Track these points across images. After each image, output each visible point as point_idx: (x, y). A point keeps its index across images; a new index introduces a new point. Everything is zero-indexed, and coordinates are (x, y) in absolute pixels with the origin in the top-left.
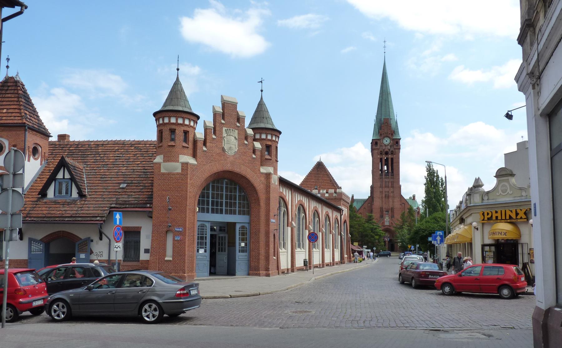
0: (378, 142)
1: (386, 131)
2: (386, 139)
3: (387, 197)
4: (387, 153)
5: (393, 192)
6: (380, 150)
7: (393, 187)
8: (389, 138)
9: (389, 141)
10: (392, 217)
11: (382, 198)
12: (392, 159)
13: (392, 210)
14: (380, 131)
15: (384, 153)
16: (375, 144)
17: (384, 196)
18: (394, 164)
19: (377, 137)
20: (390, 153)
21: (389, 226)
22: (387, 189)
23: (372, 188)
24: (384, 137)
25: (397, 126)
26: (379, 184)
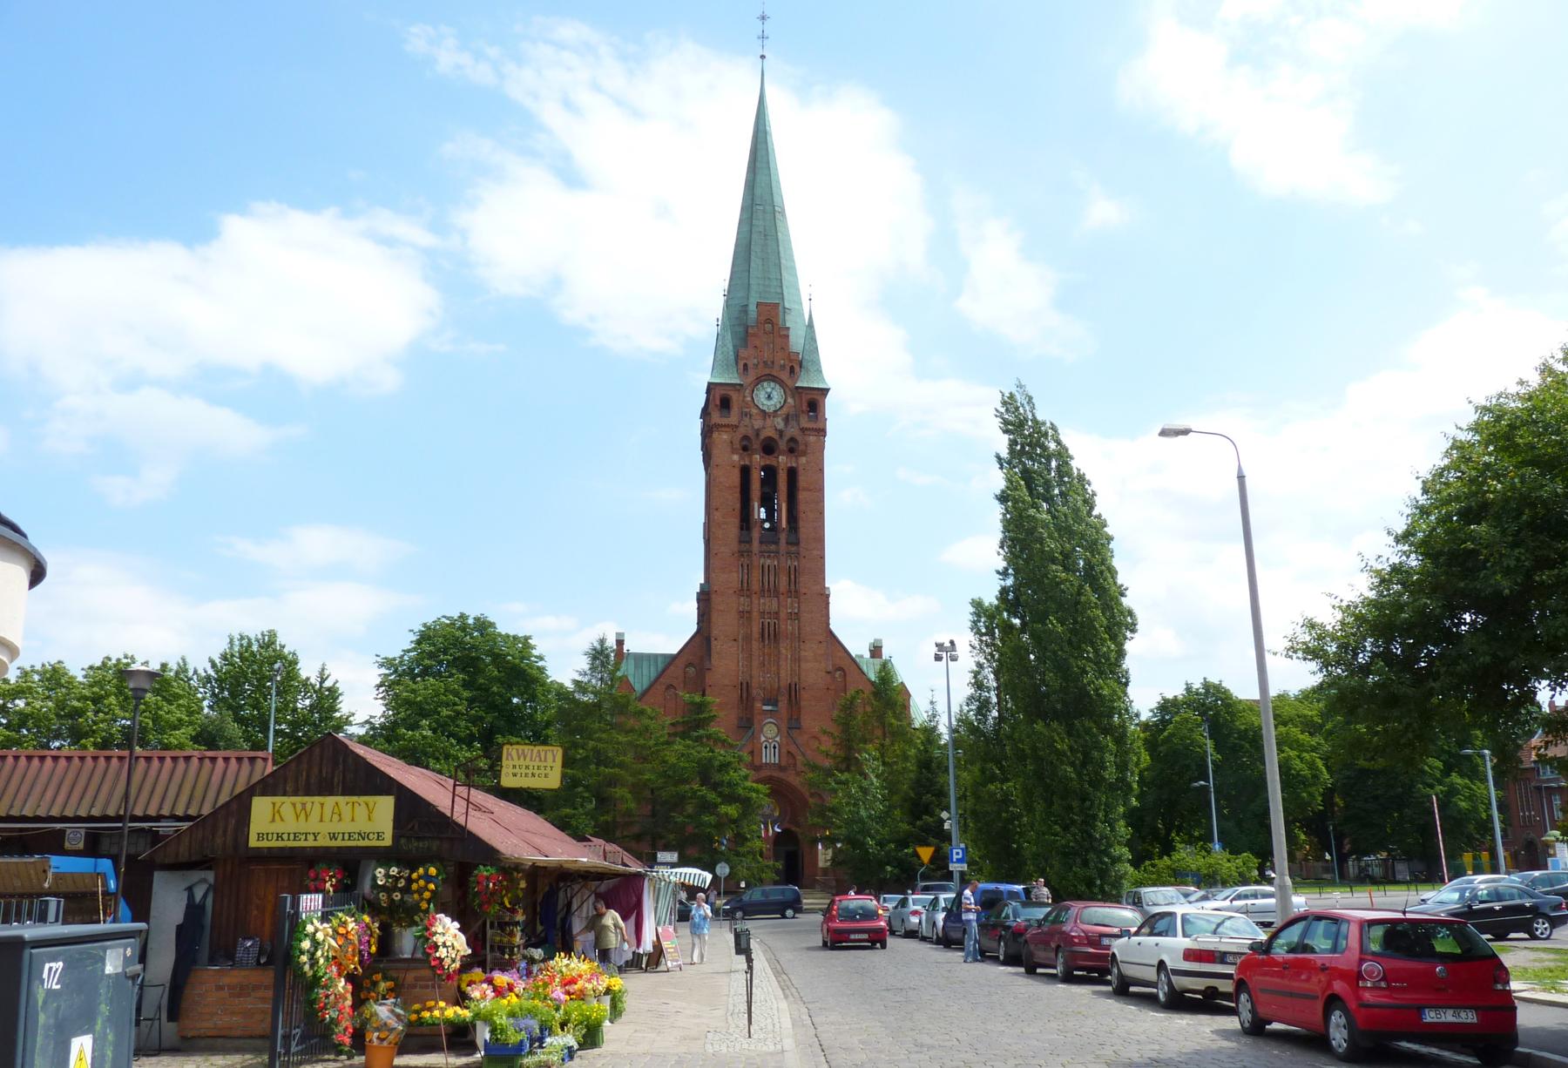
0: (734, 396)
1: (766, 355)
2: (768, 387)
3: (771, 635)
4: (769, 448)
5: (796, 616)
6: (742, 431)
7: (794, 592)
8: (782, 384)
9: (778, 395)
10: (793, 724)
11: (748, 639)
12: (792, 474)
13: (793, 692)
14: (743, 353)
15: (756, 445)
16: (719, 402)
17: (756, 629)
18: (802, 496)
19: (732, 378)
20: (783, 445)
21: (780, 767)
22: (771, 604)
23: (704, 598)
24: (759, 380)
25: (814, 340)
26: (734, 578)
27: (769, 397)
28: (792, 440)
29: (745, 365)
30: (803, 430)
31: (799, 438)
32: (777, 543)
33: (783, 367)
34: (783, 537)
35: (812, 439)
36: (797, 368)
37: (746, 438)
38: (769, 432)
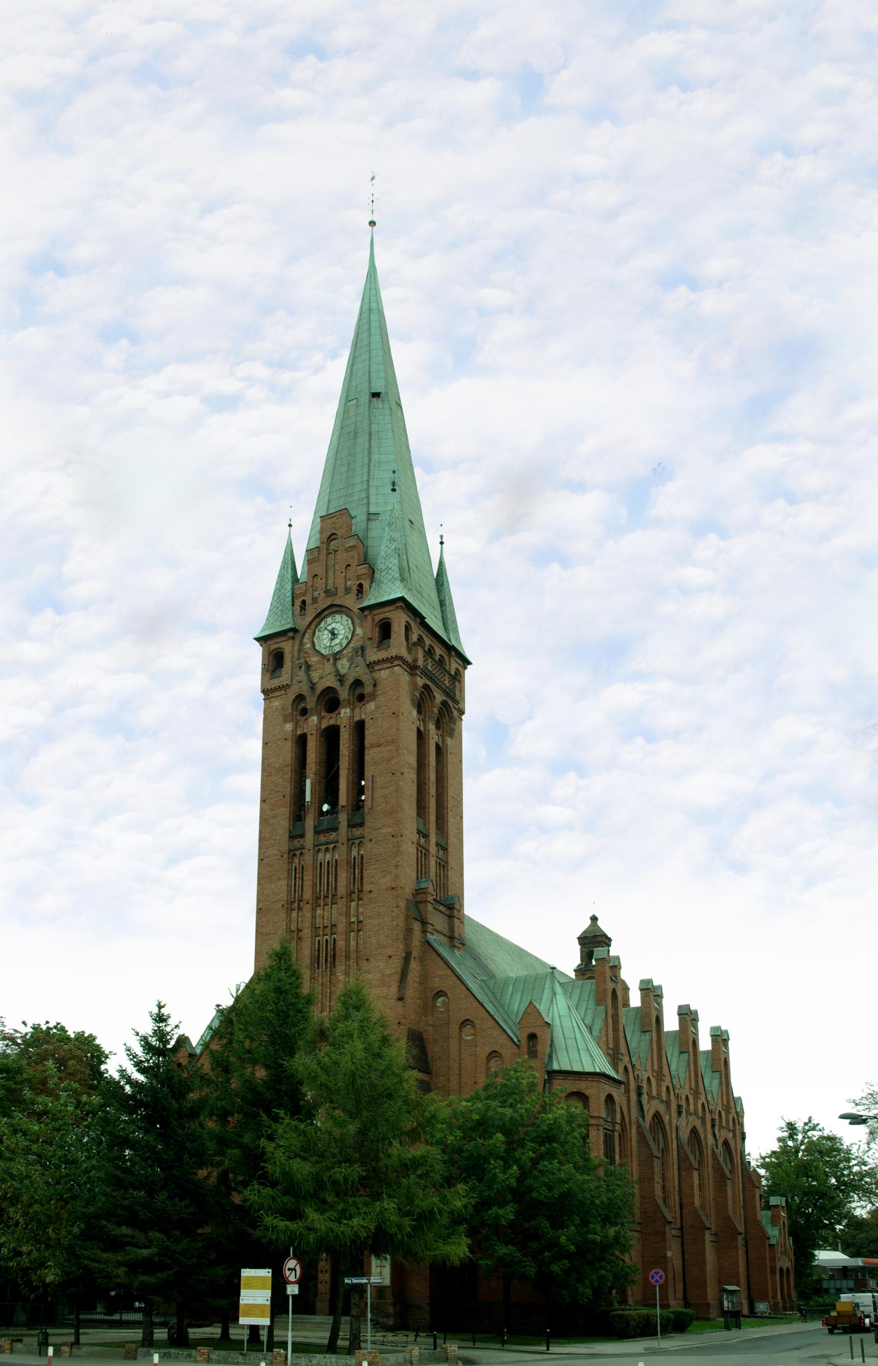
0: (287, 647)
15: (311, 703)
24: (320, 616)
27: (333, 634)
28: (358, 683)
29: (304, 602)
30: (370, 666)
31: (366, 678)
32: (335, 829)
33: (348, 590)
34: (343, 818)
35: (384, 674)
36: (366, 586)
37: (300, 698)
38: (330, 681)
